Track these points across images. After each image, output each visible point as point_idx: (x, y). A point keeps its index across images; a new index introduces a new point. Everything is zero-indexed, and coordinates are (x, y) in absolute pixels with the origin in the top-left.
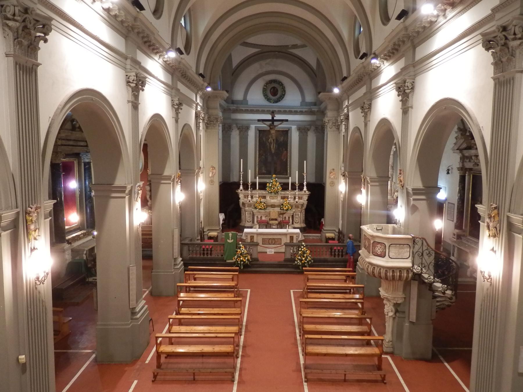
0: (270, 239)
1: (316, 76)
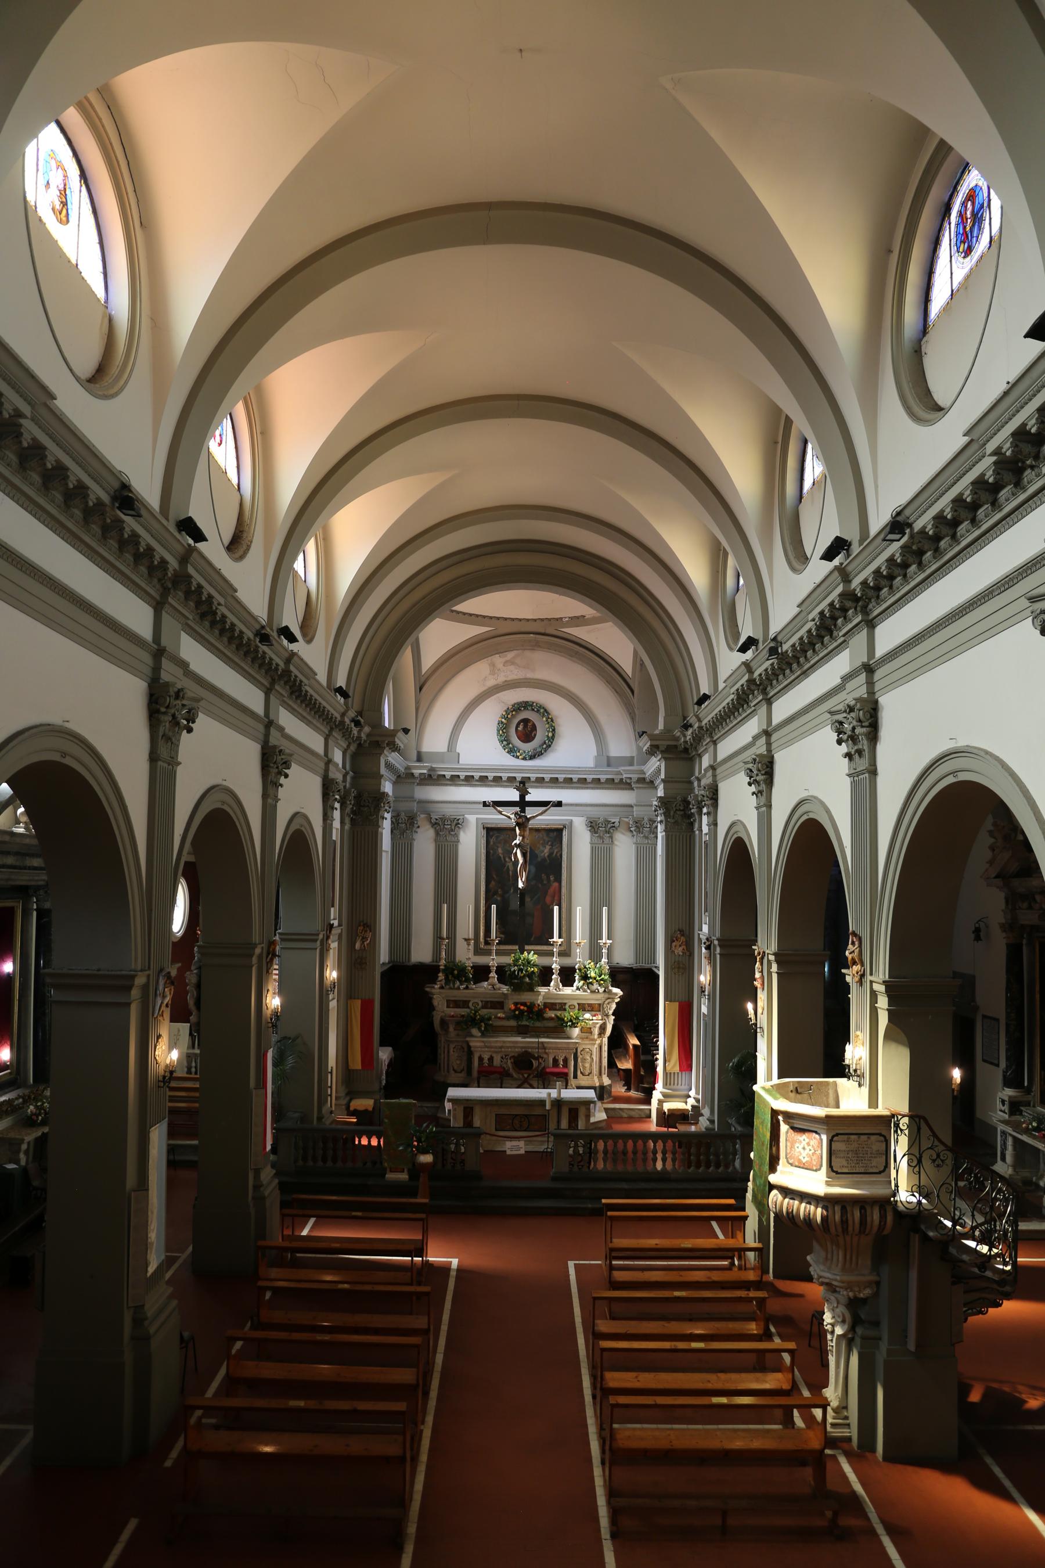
0: (517, 1115)
1: (633, 692)
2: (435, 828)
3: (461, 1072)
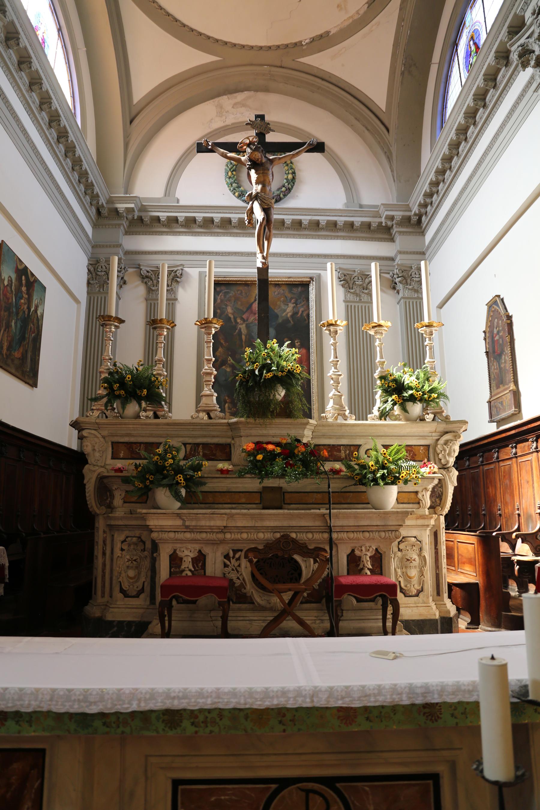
2: (146, 283)
3: (137, 596)
